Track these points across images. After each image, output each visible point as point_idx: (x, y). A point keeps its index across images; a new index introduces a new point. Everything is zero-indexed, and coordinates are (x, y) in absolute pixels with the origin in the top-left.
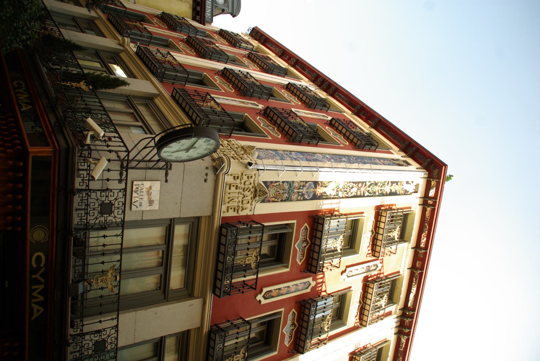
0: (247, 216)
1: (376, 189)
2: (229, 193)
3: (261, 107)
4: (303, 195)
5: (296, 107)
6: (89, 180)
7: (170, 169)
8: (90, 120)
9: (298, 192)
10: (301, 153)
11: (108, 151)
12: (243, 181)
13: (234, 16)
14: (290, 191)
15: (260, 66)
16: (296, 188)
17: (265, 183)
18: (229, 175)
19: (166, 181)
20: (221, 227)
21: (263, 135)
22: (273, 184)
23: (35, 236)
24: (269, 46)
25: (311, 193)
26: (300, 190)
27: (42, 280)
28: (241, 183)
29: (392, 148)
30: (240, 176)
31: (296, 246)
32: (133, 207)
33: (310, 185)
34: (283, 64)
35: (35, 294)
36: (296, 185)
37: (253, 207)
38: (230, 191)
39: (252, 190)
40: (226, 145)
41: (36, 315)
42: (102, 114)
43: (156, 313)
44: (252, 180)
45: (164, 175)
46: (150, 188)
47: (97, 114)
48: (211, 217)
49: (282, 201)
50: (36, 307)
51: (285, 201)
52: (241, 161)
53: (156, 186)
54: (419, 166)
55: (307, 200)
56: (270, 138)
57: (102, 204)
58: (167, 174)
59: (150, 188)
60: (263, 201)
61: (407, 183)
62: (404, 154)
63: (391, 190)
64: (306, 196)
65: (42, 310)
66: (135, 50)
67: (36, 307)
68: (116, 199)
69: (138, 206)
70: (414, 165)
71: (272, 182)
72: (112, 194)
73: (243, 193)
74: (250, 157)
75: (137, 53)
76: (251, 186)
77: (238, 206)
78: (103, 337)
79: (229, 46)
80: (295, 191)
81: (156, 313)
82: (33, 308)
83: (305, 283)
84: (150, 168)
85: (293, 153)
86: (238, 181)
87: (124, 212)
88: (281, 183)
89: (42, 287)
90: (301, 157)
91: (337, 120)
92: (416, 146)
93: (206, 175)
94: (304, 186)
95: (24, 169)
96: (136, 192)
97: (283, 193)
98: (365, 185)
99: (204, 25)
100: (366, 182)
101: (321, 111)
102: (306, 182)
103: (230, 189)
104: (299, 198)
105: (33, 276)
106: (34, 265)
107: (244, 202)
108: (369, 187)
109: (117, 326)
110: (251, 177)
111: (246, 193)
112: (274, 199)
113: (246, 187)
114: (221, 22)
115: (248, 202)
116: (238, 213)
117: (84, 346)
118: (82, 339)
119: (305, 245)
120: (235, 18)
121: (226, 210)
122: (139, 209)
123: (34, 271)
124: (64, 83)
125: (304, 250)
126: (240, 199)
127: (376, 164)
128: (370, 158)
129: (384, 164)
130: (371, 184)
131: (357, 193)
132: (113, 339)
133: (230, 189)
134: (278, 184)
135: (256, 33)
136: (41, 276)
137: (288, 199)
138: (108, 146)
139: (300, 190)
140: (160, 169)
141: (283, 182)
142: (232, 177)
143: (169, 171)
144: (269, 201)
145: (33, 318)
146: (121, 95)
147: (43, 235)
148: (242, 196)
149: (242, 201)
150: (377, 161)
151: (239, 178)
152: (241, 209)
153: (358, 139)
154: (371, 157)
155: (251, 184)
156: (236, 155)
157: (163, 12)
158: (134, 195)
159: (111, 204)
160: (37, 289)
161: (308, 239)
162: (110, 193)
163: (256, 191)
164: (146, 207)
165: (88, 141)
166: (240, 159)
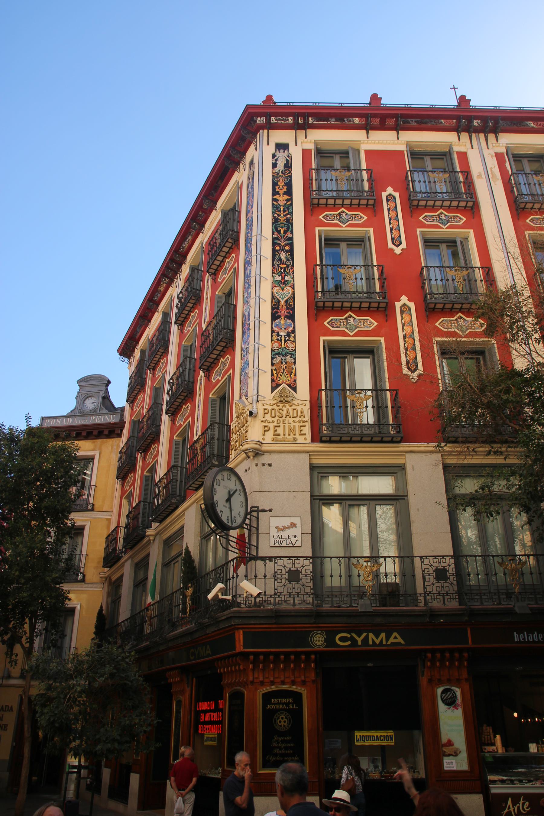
1: (282, 219)
2: (284, 435)
3: (202, 373)
4: (288, 335)
6: (265, 595)
7: (258, 507)
8: (210, 596)
9: (285, 341)
11: (237, 578)
12: (270, 419)
13: (109, 382)
14: (284, 353)
15: (161, 356)
16: (280, 345)
17: (273, 389)
18: (263, 439)
19: (270, 510)
20: (322, 441)
21: (228, 379)
23: (319, 643)
24: (139, 334)
26: (283, 339)
27: (364, 635)
28: (273, 422)
29: (237, 182)
30: (264, 424)
31: (351, 334)
33: (277, 326)
35: (377, 641)
36: (276, 346)
38: (282, 436)
39: (281, 405)
40: (236, 436)
41: (400, 640)
42: (210, 578)
43: (418, 510)
44: (270, 408)
46: (277, 528)
47: (210, 583)
48: (311, 454)
49: (295, 363)
50: (392, 640)
51: (295, 359)
53: (275, 522)
54: (252, 147)
55: (294, 327)
57: (290, 580)
58: (263, 511)
59: (277, 528)
60: (295, 389)
61: (274, 165)
62: (241, 166)
63: (285, 193)
64: (290, 329)
65: (395, 634)
66: (157, 524)
67: (392, 640)
68: (284, 567)
69: (297, 539)
70: (251, 153)
71: (273, 380)
72: (279, 571)
73: (284, 418)
75: (161, 522)
78: (431, 572)
79: (144, 392)
80: (283, 346)
81: (418, 510)
82: (392, 643)
83: (402, 312)
85: (243, 346)
86: (271, 426)
87: (297, 558)
88: (274, 368)
89: (371, 635)
91: (210, 264)
92: (229, 150)
93: (264, 465)
94: (278, 335)
95: (256, 654)
96: (281, 543)
97: (286, 363)
98: (277, 239)
99: (125, 422)
100: (273, 239)
102: (273, 332)
103: (279, 435)
105: (360, 643)
106: (349, 643)
107: (295, 415)
108: (279, 232)
109: (421, 557)
110: (265, 409)
111: (284, 413)
112: (293, 375)
114: (119, 396)
115: (294, 409)
116: (307, 422)
117: (439, 591)
118: (430, 593)
119: (352, 319)
120: (110, 380)
121: (304, 437)
123: (354, 642)
124: (188, 611)
125: (359, 320)
126: (292, 419)
131: (287, 251)
132: (435, 560)
133: (279, 435)
134: (275, 372)
135: (126, 350)
136: (359, 637)
137: (292, 353)
138: (233, 578)
139: (283, 339)
140: (258, 518)
141: (273, 364)
142: (266, 433)
143: (260, 509)
144: (295, 381)
145: (403, 642)
146: (201, 546)
147: (319, 636)
150: (249, 215)
151: (267, 424)
152: (302, 418)
153: (227, 241)
155: (273, 409)
156: (244, 427)
157: (117, 478)
158: (284, 544)
159: (290, 572)
160: (373, 639)
161: (344, 317)
162: (279, 573)
163: (281, 401)
164: (296, 531)
165: (229, 597)
166: (248, 423)
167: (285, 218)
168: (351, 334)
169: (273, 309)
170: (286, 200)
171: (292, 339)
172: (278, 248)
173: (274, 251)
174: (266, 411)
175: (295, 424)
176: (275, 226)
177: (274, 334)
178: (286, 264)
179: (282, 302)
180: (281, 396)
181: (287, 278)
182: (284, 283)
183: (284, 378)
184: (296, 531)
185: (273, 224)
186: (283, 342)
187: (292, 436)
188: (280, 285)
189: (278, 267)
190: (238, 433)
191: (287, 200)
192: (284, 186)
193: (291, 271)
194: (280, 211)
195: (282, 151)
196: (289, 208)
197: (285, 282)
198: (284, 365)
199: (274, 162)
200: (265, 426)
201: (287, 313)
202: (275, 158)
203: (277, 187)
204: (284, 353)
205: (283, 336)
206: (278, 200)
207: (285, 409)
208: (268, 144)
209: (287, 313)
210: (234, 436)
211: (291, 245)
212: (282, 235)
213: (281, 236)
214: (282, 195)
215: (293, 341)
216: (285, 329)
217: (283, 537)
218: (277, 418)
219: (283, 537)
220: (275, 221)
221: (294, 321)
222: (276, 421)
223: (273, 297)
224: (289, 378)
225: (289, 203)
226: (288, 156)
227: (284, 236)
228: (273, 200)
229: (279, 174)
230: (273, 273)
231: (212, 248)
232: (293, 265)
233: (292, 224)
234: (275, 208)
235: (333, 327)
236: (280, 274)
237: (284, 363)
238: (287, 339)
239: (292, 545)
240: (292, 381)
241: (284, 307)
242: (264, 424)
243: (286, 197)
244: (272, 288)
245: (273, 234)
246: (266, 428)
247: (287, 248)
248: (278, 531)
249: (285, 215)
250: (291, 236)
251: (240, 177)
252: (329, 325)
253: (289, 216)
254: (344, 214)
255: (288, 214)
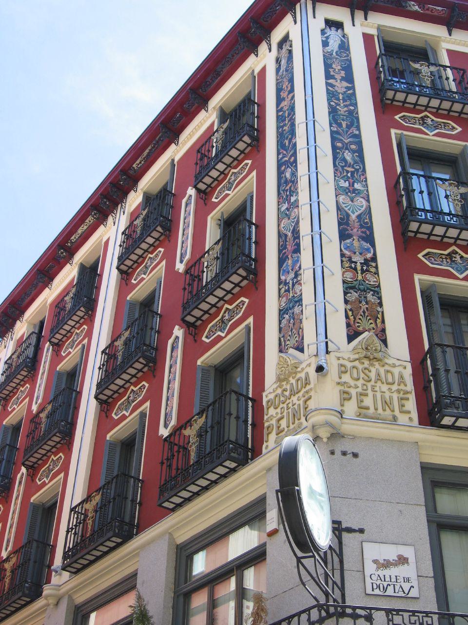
0: (415, 374)
1: (342, 110)
2: (376, 409)
3: (178, 332)
4: (366, 262)
5: (170, 259)
9: (363, 271)
10: (281, 261)
12: (352, 383)
17: (350, 338)
19: (361, 531)
22: (352, 322)
25: (361, 247)
26: (359, 268)
30: (342, 388)
31: (461, 276)
32: (414, 593)
34: (68, 275)
36: (349, 276)
37: (398, 363)
38: (372, 410)
39: (366, 362)
44: (349, 365)
45: (350, 535)
46: (375, 561)
49: (381, 304)
51: (380, 298)
52: (312, 386)
53: (373, 552)
54: (289, 18)
55: (375, 254)
56: (251, 320)
58: (349, 530)
59: (375, 561)
61: (325, 44)
62: (263, 48)
63: (343, 79)
64: (369, 256)
69: (410, 585)
70: (287, 26)
71: (348, 325)
73: (372, 383)
74: (303, 365)
76: (360, 367)
77: (398, 391)
80: (360, 278)
84: (341, 562)
86: (353, 392)
88: (349, 307)
90: (290, 262)
93: (344, 453)
94: (350, 260)
96: (385, 590)
97: (367, 303)
98: (337, 133)
100: (332, 132)
101: (176, 208)
102: (342, 255)
104: (373, 270)
107: (390, 380)
108: (340, 125)
110: (342, 365)
111: (373, 375)
112: (379, 321)
113: (362, 375)
115: (388, 371)
116: (411, 393)
121: (408, 416)
122: (415, 583)
126: (385, 388)
127: (292, 108)
128: (280, 119)
129: (292, 90)
130: (336, 123)
131: (353, 152)
133: (367, 408)
134: (350, 313)
137: (376, 290)
139: (359, 268)
141: (346, 302)
142: (346, 403)
143: (344, 526)
148: (379, 382)
149: (387, 384)
152: (402, 387)
154: (278, 117)
155: (354, 367)
156: (301, 394)
158: (390, 591)
163: (365, 357)
166: (308, 387)
167: (346, 109)
168: (461, 276)
169: (340, 224)
170: (345, 88)
171: (373, 270)
172: (339, 145)
173: (334, 148)
174: (343, 369)
175: (391, 394)
176: (333, 117)
177: (344, 259)
178: (353, 167)
179: (353, 217)
180: (367, 349)
181: (357, 186)
182: (354, 192)
183: (365, 324)
184: (408, 571)
185: (330, 113)
186: (359, 272)
187: (388, 412)
188: (347, 193)
189: (343, 169)
190: (281, 405)
191: (348, 88)
192: (341, 70)
193: (362, 177)
194: (339, 100)
195: (333, 29)
196: (351, 97)
197: (354, 191)
198: (364, 306)
199: (324, 39)
200: (345, 392)
201: (362, 232)
202: (325, 35)
203: (331, 70)
204: (362, 287)
205: (358, 264)
206: (335, 86)
207: (373, 370)
208: (314, 17)
209: (362, 232)
210: (272, 411)
211: (360, 144)
212: (345, 130)
213: (343, 130)
214: (339, 81)
215: (375, 274)
216: (361, 254)
217: (388, 579)
218: (361, 382)
219: (388, 579)
220: (333, 111)
221: (373, 245)
222: (360, 386)
223: (339, 208)
224: (373, 325)
225: (350, 92)
226: (344, 36)
227: (347, 132)
228: (327, 84)
229: (332, 54)
230: (335, 176)
231: (201, 159)
232: (364, 170)
233: (358, 119)
234: (331, 95)
235: (432, 263)
236: (346, 179)
237: (364, 303)
238: (365, 268)
239: (403, 595)
240: (379, 330)
241: (357, 225)
242: (342, 388)
243: (345, 84)
244: (336, 196)
245: (331, 125)
246: (346, 396)
247: (353, 147)
248: (378, 568)
249: (346, 106)
250: (357, 132)
251: (264, 59)
252: (426, 258)
253: (352, 108)
254: (429, 119)
255: (351, 105)
